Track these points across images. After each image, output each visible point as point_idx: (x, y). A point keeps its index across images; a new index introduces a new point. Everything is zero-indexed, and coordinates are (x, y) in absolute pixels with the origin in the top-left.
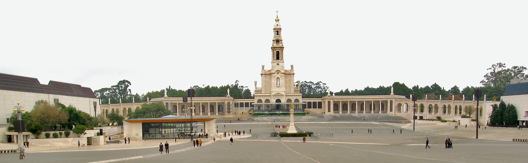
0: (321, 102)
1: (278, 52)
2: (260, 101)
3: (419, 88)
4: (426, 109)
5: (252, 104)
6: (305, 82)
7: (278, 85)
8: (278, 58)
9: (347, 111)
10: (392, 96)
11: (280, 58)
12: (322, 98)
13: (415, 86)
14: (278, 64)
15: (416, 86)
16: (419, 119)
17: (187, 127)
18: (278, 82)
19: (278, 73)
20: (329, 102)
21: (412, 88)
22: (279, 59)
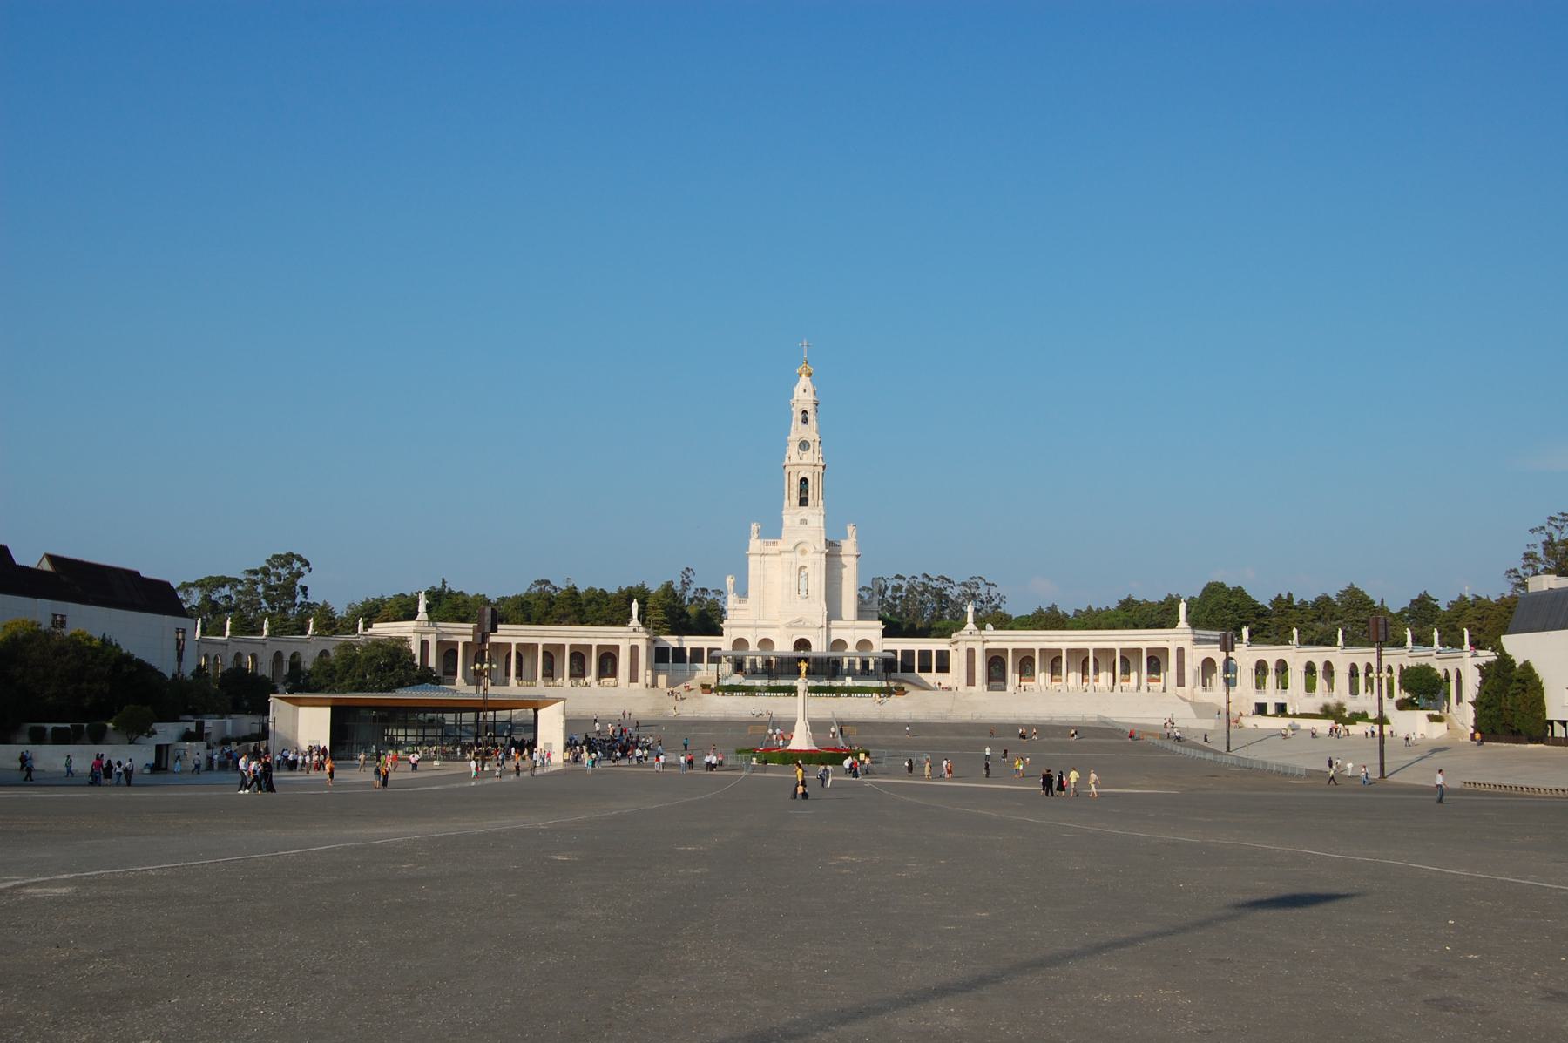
0: (948, 652)
1: (804, 481)
2: (740, 643)
3: (1295, 603)
4: (1296, 677)
5: (715, 653)
6: (926, 576)
7: (803, 593)
8: (803, 502)
9: (1005, 684)
10: (1181, 631)
11: (810, 502)
12: (951, 637)
13: (1280, 595)
14: (804, 522)
15: (1285, 597)
16: (1274, 713)
17: (461, 721)
18: (803, 581)
19: (803, 552)
20: (971, 652)
21: (1270, 604)
22: (807, 505)
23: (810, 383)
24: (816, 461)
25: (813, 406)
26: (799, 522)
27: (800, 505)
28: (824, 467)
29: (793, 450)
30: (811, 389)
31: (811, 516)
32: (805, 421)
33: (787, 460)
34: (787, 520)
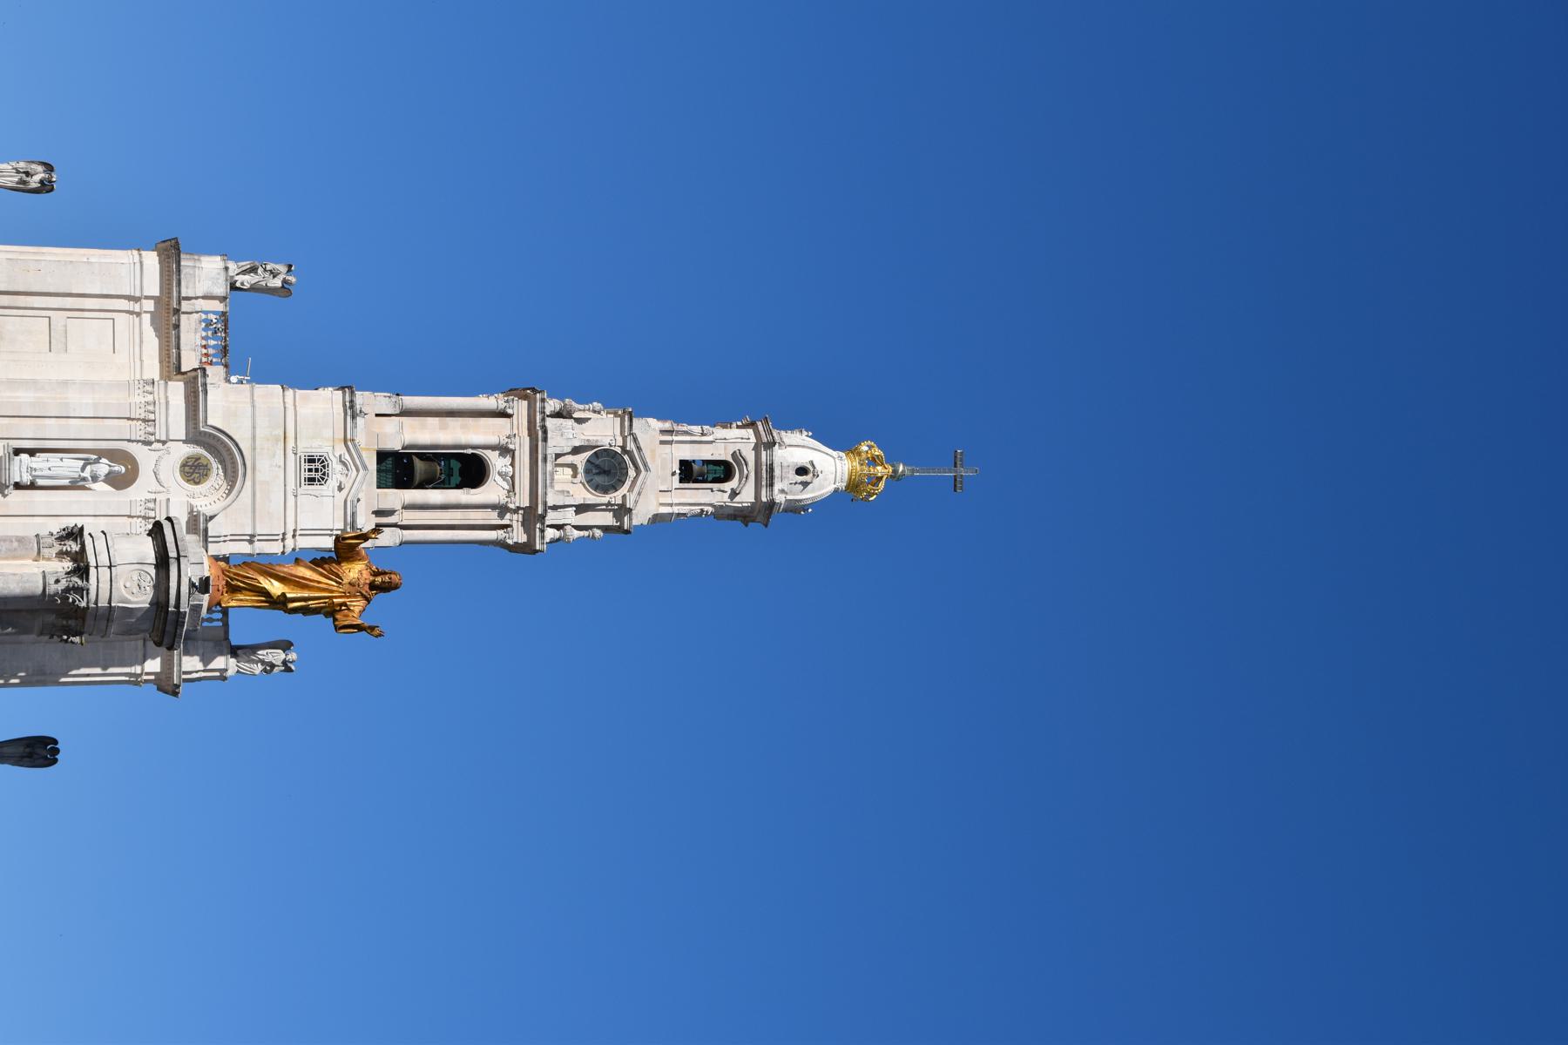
1: (470, 469)
11: (395, 498)
14: (316, 470)
19: (193, 471)
23: (829, 489)
24: (552, 517)
25: (747, 497)
26: (316, 452)
27: (382, 456)
28: (527, 549)
29: (603, 429)
30: (808, 495)
31: (341, 496)
32: (688, 472)
33: (552, 405)
34: (324, 403)
